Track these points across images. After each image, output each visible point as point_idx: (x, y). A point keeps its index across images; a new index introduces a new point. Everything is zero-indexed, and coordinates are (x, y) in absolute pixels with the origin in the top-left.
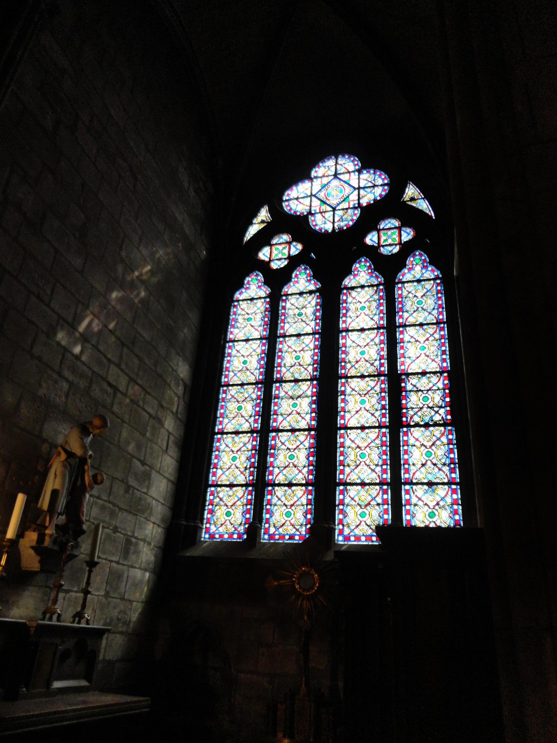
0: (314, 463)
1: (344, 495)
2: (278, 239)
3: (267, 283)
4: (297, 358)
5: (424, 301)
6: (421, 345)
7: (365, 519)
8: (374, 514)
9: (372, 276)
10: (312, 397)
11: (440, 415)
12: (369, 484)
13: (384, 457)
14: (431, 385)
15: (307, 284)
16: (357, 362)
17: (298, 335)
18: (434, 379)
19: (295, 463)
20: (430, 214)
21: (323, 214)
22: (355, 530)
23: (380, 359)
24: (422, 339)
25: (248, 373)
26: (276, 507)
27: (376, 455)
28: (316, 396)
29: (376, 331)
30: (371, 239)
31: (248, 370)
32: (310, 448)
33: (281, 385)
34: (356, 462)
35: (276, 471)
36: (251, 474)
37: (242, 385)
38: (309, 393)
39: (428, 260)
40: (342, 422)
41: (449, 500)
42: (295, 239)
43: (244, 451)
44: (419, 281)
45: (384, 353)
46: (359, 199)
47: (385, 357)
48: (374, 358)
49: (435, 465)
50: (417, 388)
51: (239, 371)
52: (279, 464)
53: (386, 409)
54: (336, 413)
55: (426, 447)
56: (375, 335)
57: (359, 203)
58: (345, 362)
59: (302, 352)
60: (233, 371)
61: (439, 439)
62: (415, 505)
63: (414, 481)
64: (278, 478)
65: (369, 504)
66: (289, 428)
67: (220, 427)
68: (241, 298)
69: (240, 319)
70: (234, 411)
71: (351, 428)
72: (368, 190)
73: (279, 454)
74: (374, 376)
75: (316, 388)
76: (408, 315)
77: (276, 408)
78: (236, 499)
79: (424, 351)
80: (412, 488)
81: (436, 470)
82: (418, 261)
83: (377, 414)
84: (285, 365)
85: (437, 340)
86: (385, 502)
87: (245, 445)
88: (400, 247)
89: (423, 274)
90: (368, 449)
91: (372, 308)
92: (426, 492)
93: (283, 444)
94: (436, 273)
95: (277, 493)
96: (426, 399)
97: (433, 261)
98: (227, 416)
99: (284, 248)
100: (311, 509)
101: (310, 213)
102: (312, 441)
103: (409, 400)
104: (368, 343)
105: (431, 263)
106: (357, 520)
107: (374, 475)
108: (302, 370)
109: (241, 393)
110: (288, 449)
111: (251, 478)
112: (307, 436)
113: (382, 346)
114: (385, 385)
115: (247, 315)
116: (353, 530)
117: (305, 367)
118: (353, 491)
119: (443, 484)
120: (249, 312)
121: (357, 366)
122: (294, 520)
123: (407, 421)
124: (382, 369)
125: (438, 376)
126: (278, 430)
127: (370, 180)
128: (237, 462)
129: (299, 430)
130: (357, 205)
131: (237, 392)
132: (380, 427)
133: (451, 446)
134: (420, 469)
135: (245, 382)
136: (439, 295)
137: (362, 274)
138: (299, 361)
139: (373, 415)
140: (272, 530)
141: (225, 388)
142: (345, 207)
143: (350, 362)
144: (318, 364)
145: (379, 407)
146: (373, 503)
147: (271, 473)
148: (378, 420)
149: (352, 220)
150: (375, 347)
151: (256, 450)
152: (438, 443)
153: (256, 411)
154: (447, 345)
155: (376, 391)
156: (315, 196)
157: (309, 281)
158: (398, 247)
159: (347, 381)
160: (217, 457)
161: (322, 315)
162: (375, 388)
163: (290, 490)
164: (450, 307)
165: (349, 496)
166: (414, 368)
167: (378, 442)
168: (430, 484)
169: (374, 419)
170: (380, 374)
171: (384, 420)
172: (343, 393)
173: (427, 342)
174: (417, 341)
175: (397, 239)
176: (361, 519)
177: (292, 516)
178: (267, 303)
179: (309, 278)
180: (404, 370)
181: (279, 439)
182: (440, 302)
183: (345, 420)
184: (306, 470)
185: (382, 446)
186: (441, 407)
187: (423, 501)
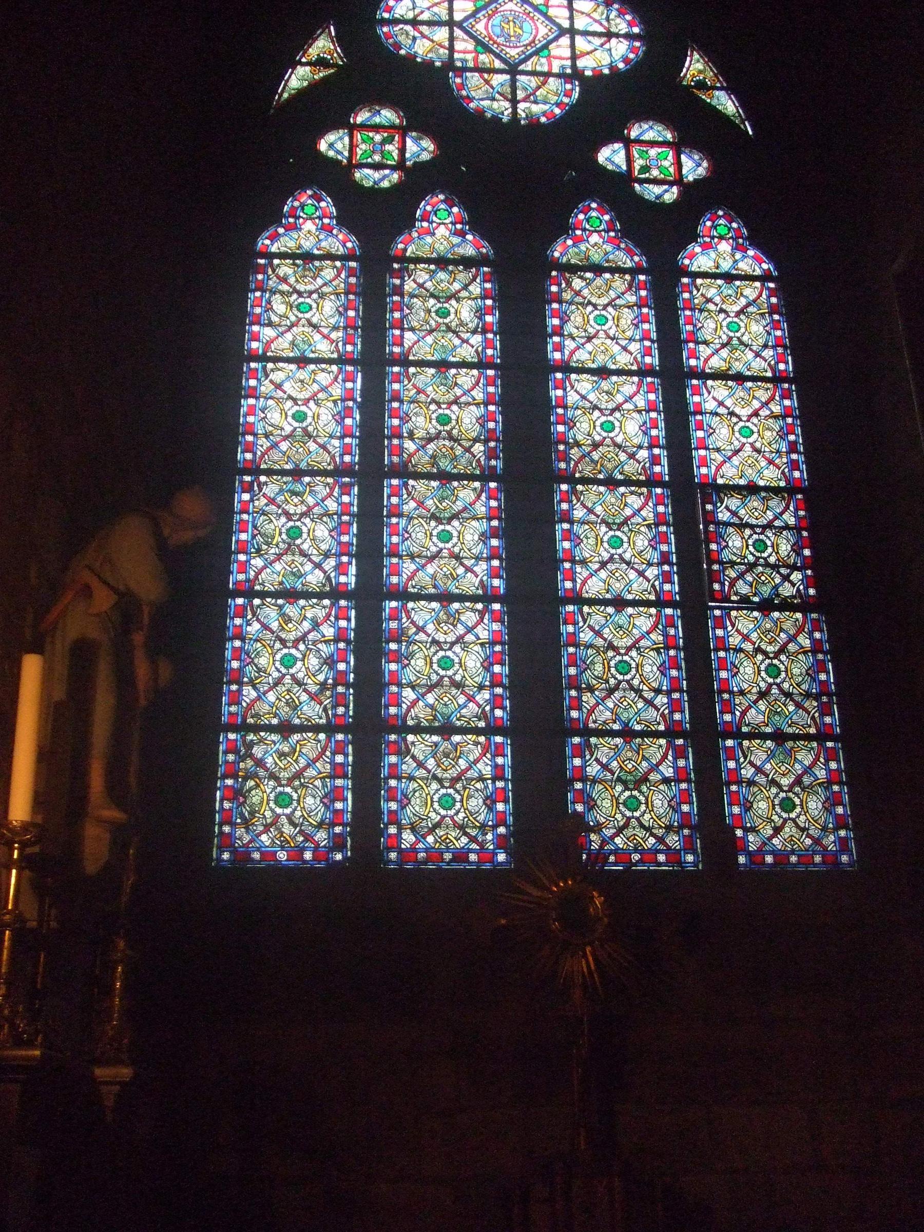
0: (505, 681)
1: (582, 756)
2: (368, 115)
3: (345, 220)
4: (444, 420)
5: (742, 325)
6: (741, 424)
7: (637, 814)
8: (657, 803)
9: (619, 248)
10: (490, 519)
11: (793, 585)
12: (643, 734)
13: (674, 673)
14: (770, 515)
15: (456, 240)
16: (596, 446)
17: (442, 365)
18: (776, 504)
19: (458, 678)
20: (742, 126)
21: (486, 76)
22: (618, 840)
23: (650, 447)
24: (744, 412)
25: (312, 446)
26: (413, 785)
27: (655, 669)
28: (500, 519)
29: (636, 379)
30: (611, 156)
31: (310, 436)
32: (493, 643)
33: (406, 485)
34: (607, 681)
35: (409, 694)
36: (340, 700)
37: (297, 474)
38: (481, 509)
39: (745, 231)
40: (568, 585)
41: (821, 774)
42: (416, 122)
43: (315, 643)
44: (729, 278)
45: (658, 432)
46: (574, 57)
47: (662, 441)
48: (636, 441)
49: (788, 695)
50: (742, 520)
51: (286, 438)
52: (413, 678)
53: (671, 564)
54: (554, 563)
55: (765, 653)
56: (634, 388)
57: (574, 66)
58: (566, 443)
59: (455, 408)
60: (267, 436)
61: (792, 639)
62: (751, 783)
63: (745, 729)
64: (412, 713)
65: (645, 779)
66: (433, 591)
67: (241, 577)
68: (274, 249)
69: (279, 305)
70: (277, 538)
71: (591, 602)
72: (597, 41)
73: (410, 656)
74: (639, 484)
75: (496, 499)
76: (709, 351)
77: (395, 539)
78: (303, 762)
79: (751, 440)
80: (740, 745)
81: (791, 708)
82: (722, 230)
83: (652, 572)
84: (411, 436)
85: (776, 417)
86: (680, 776)
87: (316, 625)
88: (679, 191)
89: (736, 262)
90: (634, 653)
91: (623, 322)
92: (771, 756)
93: (421, 629)
94: (765, 266)
95: (415, 751)
96: (760, 545)
97: (757, 237)
98: (258, 551)
99: (390, 140)
100: (503, 789)
101: (449, 65)
102: (496, 626)
103: (724, 544)
104: (621, 405)
105: (755, 240)
106: (619, 816)
107: (652, 714)
108: (459, 451)
109: (296, 494)
110: (435, 642)
111: (340, 710)
112: (482, 614)
113: (653, 415)
114: (666, 506)
115: (295, 296)
116: (612, 838)
117: (466, 444)
118: (604, 748)
119: (808, 737)
120: (300, 287)
121: (596, 456)
122: (461, 815)
123: (722, 590)
124: (657, 469)
125: (783, 498)
126: (403, 595)
127: (596, 16)
128: (298, 669)
129: (462, 598)
130: (569, 71)
131: (281, 491)
132: (660, 603)
133: (820, 656)
134: (755, 702)
135: (303, 465)
136: (776, 317)
137: (593, 236)
138: (448, 428)
139: (641, 574)
140: (408, 838)
141: (247, 478)
142: (539, 68)
143: (577, 444)
144: (497, 440)
145: (655, 557)
146: (654, 777)
147: (397, 701)
148: (653, 586)
149: (558, 105)
150: (635, 415)
151: (348, 642)
152: (792, 647)
153: (340, 543)
154: (799, 430)
155: (645, 520)
156: (460, 25)
157: (461, 234)
158: (675, 189)
159: (574, 491)
160: (237, 654)
161: (500, 321)
162: (644, 513)
163: (446, 744)
164: (798, 344)
165: (597, 760)
166: (729, 474)
167: (656, 637)
168: (779, 737)
169: (646, 585)
170: (652, 482)
171: (667, 587)
172: (567, 517)
173: (754, 420)
174: (732, 414)
175: (672, 170)
176: (628, 814)
177: (458, 805)
178: (351, 272)
179: (459, 226)
180: (707, 476)
181: (409, 617)
182: (779, 333)
183: (574, 581)
184: (486, 695)
185: (667, 648)
186: (794, 568)
187: (767, 776)
